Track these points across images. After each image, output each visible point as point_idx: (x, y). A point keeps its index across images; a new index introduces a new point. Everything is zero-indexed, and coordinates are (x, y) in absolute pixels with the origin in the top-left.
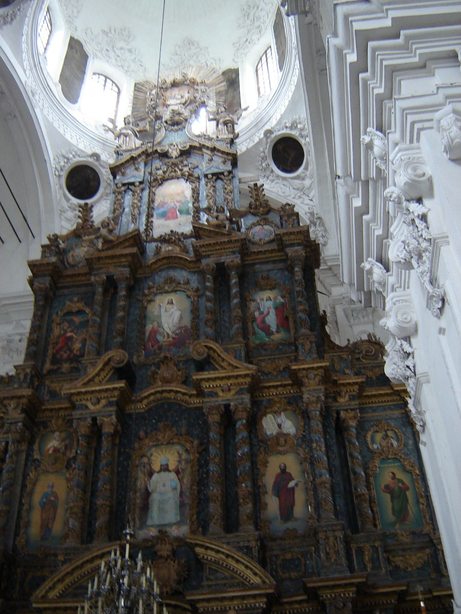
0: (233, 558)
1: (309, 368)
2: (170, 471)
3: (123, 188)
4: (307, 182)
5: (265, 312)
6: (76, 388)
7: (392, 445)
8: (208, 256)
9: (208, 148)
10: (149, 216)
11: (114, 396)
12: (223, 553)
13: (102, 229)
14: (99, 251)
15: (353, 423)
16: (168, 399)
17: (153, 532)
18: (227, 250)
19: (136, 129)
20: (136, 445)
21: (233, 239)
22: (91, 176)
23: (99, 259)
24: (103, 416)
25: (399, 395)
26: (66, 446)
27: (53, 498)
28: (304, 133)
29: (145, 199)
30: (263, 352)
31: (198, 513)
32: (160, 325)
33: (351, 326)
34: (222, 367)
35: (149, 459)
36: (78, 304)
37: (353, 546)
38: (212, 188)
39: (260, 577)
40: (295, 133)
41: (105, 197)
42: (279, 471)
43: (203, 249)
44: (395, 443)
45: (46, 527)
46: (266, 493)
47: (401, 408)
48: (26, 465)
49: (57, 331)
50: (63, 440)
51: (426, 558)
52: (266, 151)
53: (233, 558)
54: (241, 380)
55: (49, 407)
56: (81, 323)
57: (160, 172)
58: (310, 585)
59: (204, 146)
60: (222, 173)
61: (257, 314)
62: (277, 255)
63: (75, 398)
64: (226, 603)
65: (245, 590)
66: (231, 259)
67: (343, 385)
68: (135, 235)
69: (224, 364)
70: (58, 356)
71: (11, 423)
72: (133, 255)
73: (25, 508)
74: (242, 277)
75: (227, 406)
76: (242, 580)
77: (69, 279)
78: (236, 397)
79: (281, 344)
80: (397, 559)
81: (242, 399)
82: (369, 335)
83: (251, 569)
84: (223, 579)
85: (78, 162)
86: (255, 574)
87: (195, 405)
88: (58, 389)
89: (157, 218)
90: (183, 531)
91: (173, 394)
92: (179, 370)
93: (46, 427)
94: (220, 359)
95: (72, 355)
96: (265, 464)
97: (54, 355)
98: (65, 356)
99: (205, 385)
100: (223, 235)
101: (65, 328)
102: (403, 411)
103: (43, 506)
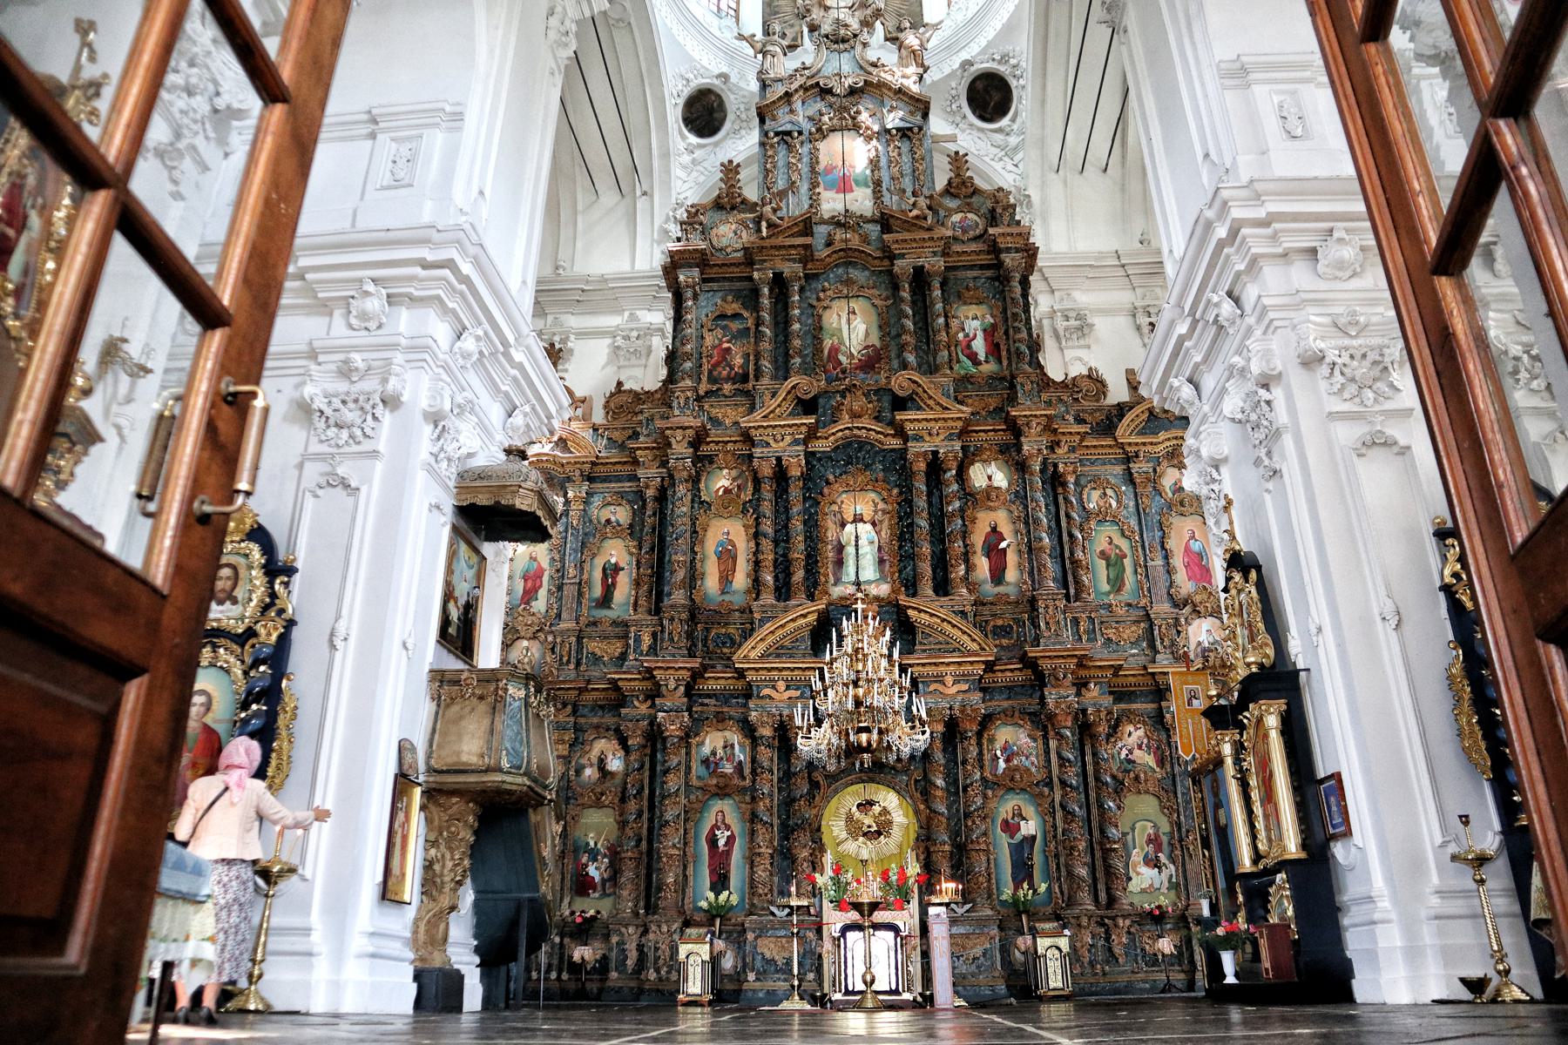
4: (1013, 140)
8: (902, 256)
10: (814, 185)
15: (1071, 479)
17: (851, 589)
19: (785, 43)
20: (826, 490)
26: (739, 487)
31: (900, 572)
32: (842, 342)
33: (1062, 350)
40: (1002, 69)
44: (1114, 504)
45: (726, 579)
49: (709, 340)
50: (734, 480)
56: (739, 331)
60: (910, 129)
61: (961, 335)
62: (985, 259)
63: (753, 432)
64: (941, 668)
66: (934, 263)
69: (931, 402)
72: (807, 247)
74: (943, 285)
75: (935, 453)
77: (715, 269)
79: (991, 377)
90: (883, 590)
96: (973, 521)
97: (710, 372)
99: (908, 426)
100: (921, 227)
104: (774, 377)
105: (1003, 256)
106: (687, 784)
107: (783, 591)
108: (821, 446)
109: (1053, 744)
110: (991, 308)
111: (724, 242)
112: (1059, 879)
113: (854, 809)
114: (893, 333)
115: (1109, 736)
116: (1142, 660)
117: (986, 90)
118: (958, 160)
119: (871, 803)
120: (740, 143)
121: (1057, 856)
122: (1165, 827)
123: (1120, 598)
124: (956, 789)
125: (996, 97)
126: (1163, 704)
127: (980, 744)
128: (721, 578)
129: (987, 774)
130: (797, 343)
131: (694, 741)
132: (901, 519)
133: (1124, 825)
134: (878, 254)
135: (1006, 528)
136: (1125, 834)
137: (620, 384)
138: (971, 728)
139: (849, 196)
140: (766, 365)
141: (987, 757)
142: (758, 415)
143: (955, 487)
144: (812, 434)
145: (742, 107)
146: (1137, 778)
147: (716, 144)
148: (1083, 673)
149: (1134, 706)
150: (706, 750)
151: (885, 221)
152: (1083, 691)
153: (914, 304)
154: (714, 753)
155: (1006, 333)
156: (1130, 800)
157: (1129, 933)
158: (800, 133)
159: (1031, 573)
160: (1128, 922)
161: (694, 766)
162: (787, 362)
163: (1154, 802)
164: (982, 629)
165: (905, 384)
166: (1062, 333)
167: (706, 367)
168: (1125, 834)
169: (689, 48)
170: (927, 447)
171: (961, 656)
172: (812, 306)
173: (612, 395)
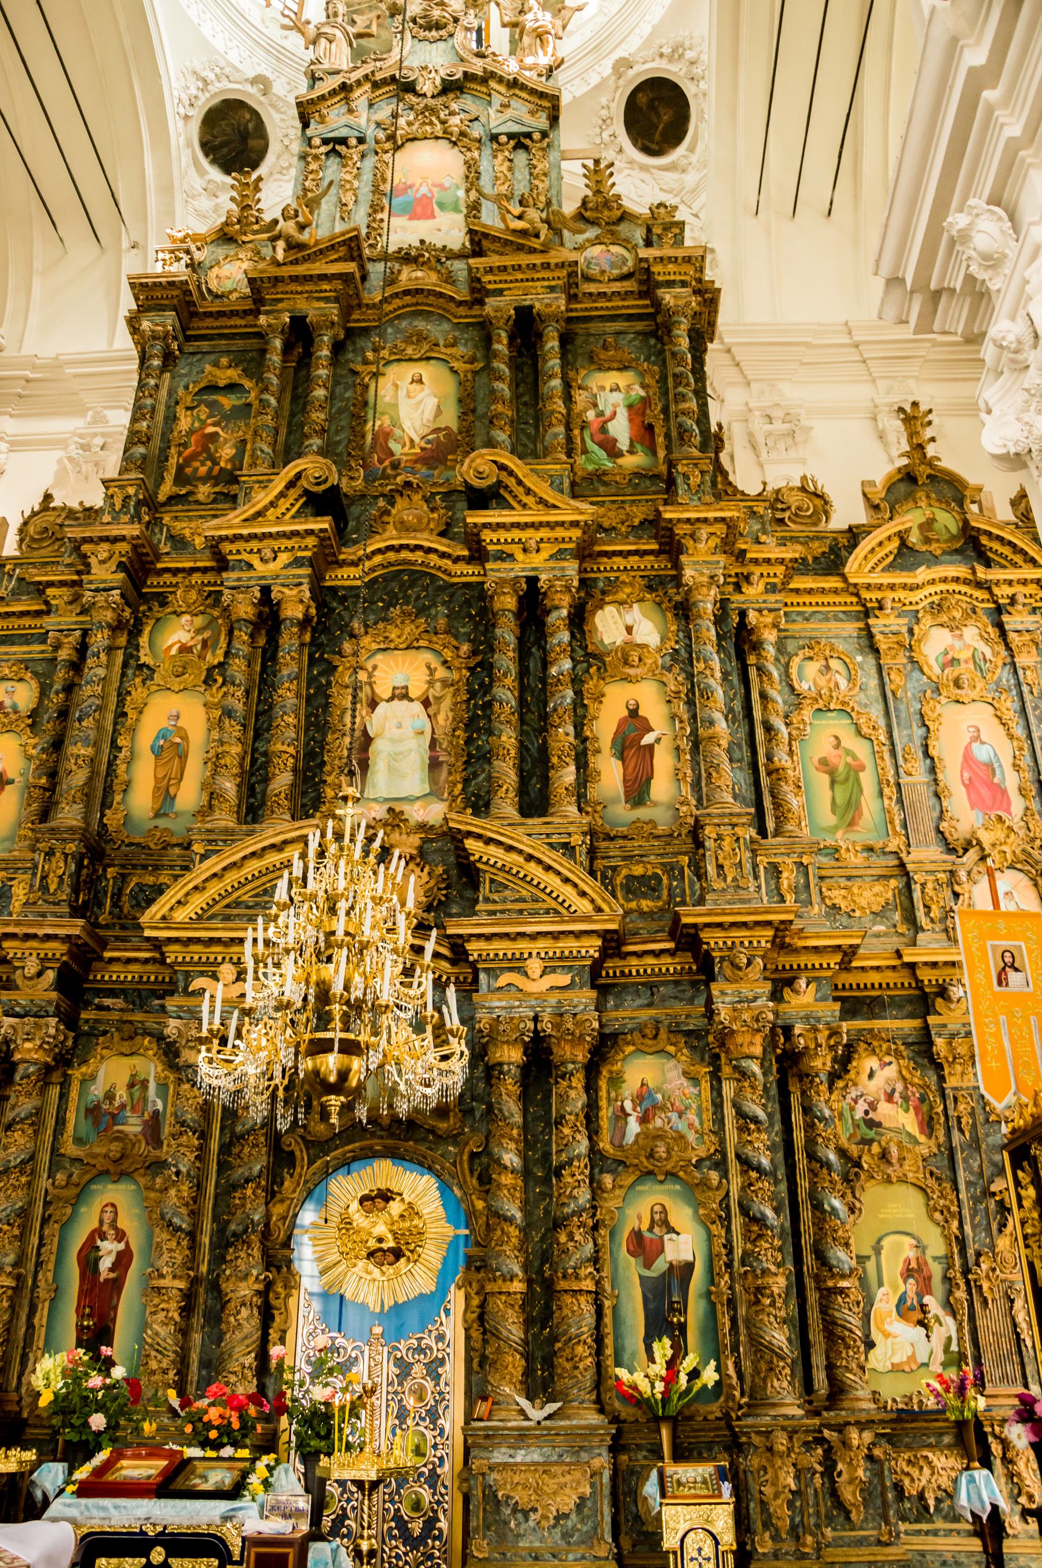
0: (539, 862)
1: (698, 520)
2: (411, 700)
3: (324, 149)
5: (608, 413)
6: (230, 527)
7: (837, 685)
8: (500, 292)
9: (501, 80)
11: (306, 548)
12: (520, 852)
13: (281, 222)
14: (279, 265)
15: (770, 636)
19: (352, 30)
20: (347, 647)
21: (553, 261)
22: (251, 126)
23: (277, 280)
25: (857, 595)
26: (205, 643)
27: (178, 740)
28: (698, 71)
29: (367, 177)
30: (602, 489)
31: (466, 781)
32: (396, 423)
33: (761, 465)
34: (524, 506)
35: (370, 676)
36: (230, 372)
37: (762, 861)
39: (592, 901)
40: (675, 72)
41: (277, 176)
42: (626, 713)
44: (843, 683)
46: (598, 751)
47: (858, 620)
48: (123, 675)
49: (184, 422)
51: (890, 895)
52: (613, 105)
53: (539, 862)
54: (560, 533)
58: (685, 920)
60: (528, 135)
61: (591, 415)
63: (226, 547)
64: (523, 945)
65: (563, 922)
66: (548, 301)
67: (756, 561)
69: (529, 500)
71: (97, 590)
72: (345, 278)
73: (121, 756)
74: (566, 340)
76: (554, 904)
77: (209, 322)
78: (551, 564)
79: (636, 474)
80: (834, 893)
81: (563, 569)
82: (804, 478)
83: (575, 886)
84: (516, 901)
85: (222, 92)
86: (583, 894)
88: (187, 533)
90: (434, 812)
91: (420, 553)
92: (432, 510)
93: (164, 604)
94: (521, 489)
95: (217, 469)
96: (599, 698)
97: (180, 468)
98: (203, 470)
99: (487, 536)
102: (861, 625)
103: (158, 752)
105: (660, 292)
106: (54, 1150)
107: (253, 809)
109: (728, 1089)
110: (642, 374)
111: (228, 285)
112: (735, 1348)
113: (355, 1205)
115: (834, 1077)
116: (895, 942)
117: (652, 106)
118: (598, 173)
119: (386, 1196)
121: (732, 1303)
122: (936, 1246)
123: (853, 837)
124: (542, 1171)
125: (666, 116)
126: (932, 1020)
127: (591, 1088)
128: (157, 789)
129: (605, 1144)
130: (318, 416)
131: (77, 1073)
132: (472, 694)
133: (861, 1244)
135: (654, 711)
136: (862, 1259)
137: (48, 497)
138: (574, 1055)
141: (606, 1113)
143: (565, 636)
146: (884, 1155)
148: (786, 960)
149: (877, 1024)
150: (97, 1091)
152: (787, 991)
154: (110, 1096)
155: (665, 410)
156: (871, 1193)
157: (870, 1458)
159: (696, 786)
160: (868, 1436)
161: (71, 1116)
163: (916, 1199)
164: (607, 882)
165: (486, 468)
166: (761, 440)
167: (173, 462)
168: (862, 1259)
169: (206, 30)
170: (522, 565)
171: (551, 918)
173: (34, 514)
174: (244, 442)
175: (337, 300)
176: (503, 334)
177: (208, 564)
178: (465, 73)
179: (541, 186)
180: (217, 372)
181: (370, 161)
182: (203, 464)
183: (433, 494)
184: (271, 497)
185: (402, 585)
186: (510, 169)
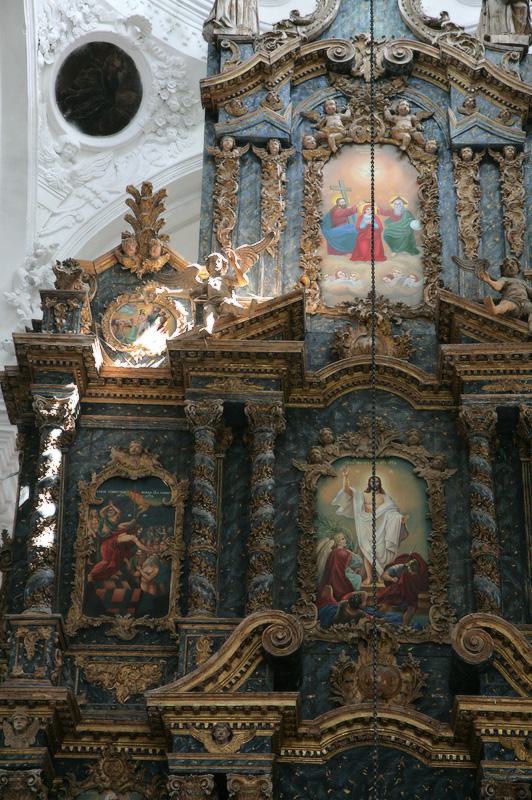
6: (179, 697)
8: (478, 387)
9: (464, 70)
11: (267, 727)
16: (382, 739)
18: (522, 378)
24: (240, 773)
32: (353, 545)
36: (144, 461)
38: (472, 186)
41: (151, 136)
43: (467, 367)
55: (94, 728)
57: (336, 120)
59: (454, 62)
60: (500, 149)
63: (171, 719)
68: (293, 304)
70: (101, 592)
71: (12, 768)
72: (292, 359)
87: (445, 764)
89: (332, 251)
92: (405, 670)
93: (83, 776)
95: (137, 592)
97: (90, 588)
98: (119, 593)
99: (484, 726)
100: (517, 334)
101: (113, 519)
104: (218, 608)
108: (308, 752)
114: (455, 533)
120: (165, 150)
130: (266, 542)
134: (430, 380)
139: (379, 266)
140: (204, 583)
142: (183, 684)
144: (289, 728)
145: (172, 84)
147: (119, 150)
151: (446, 320)
153: (496, 478)
158: (285, 144)
162: (244, 579)
165: (479, 639)
167: (79, 580)
172: (296, 471)
174: (168, 559)
175: (279, 385)
176: (484, 444)
177: (140, 729)
178: (416, 54)
179: (517, 222)
180: (129, 461)
181: (299, 170)
182: (119, 586)
183: (405, 646)
184: (225, 660)
185: (371, 767)
186: (477, 195)
